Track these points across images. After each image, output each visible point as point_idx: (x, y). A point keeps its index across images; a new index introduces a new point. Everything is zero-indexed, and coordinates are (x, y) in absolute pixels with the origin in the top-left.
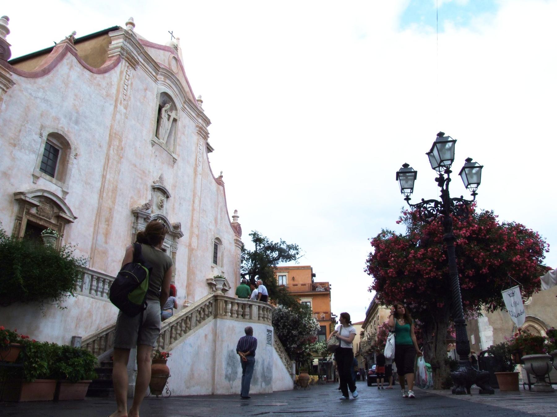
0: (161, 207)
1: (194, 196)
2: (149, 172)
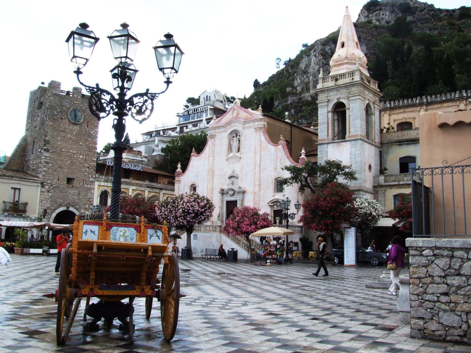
0: (233, 184)
1: (255, 166)
2: (227, 172)
